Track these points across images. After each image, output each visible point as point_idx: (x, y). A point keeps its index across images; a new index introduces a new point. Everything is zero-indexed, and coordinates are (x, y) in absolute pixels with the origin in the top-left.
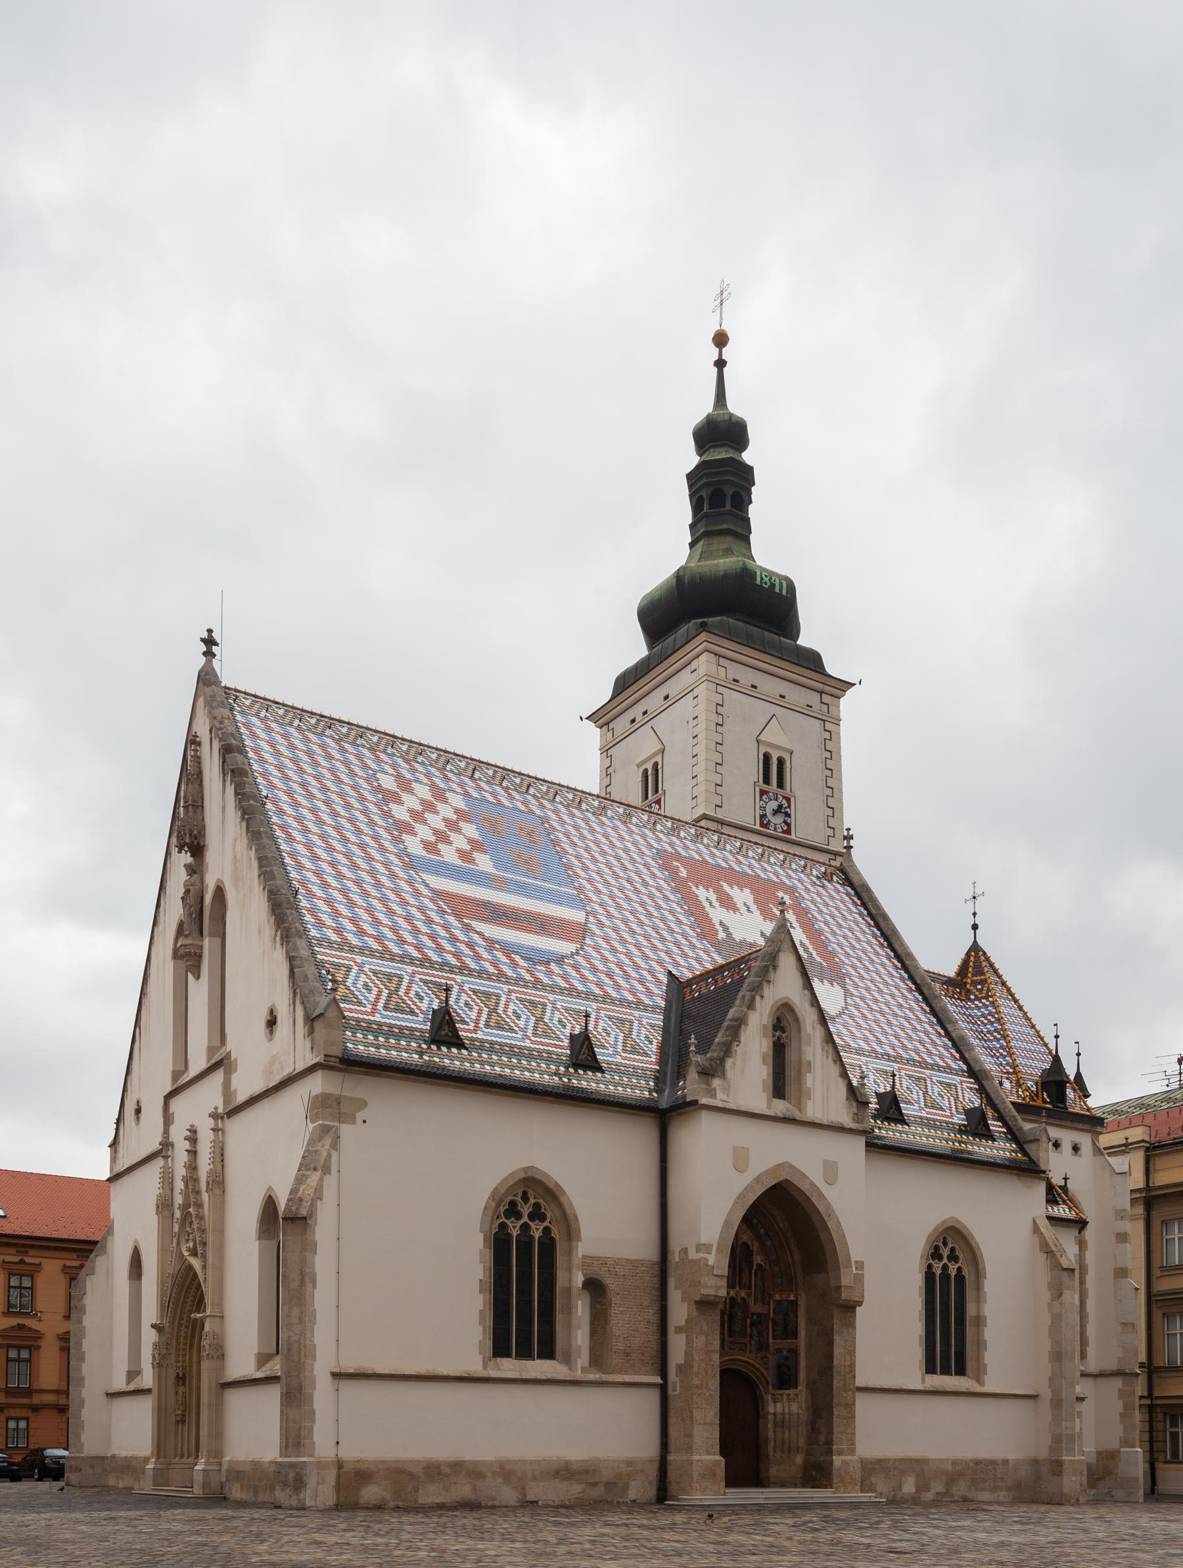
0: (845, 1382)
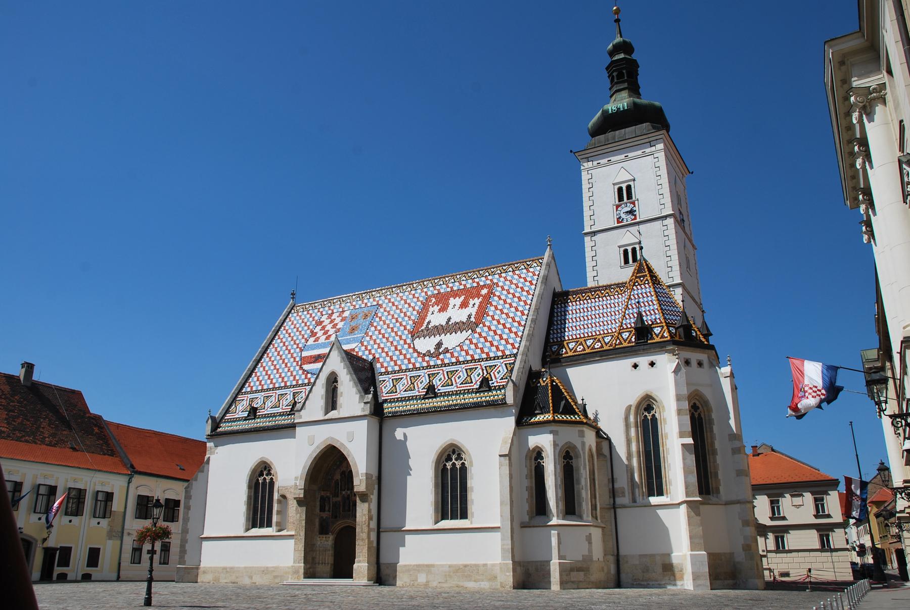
0: (362, 528)
